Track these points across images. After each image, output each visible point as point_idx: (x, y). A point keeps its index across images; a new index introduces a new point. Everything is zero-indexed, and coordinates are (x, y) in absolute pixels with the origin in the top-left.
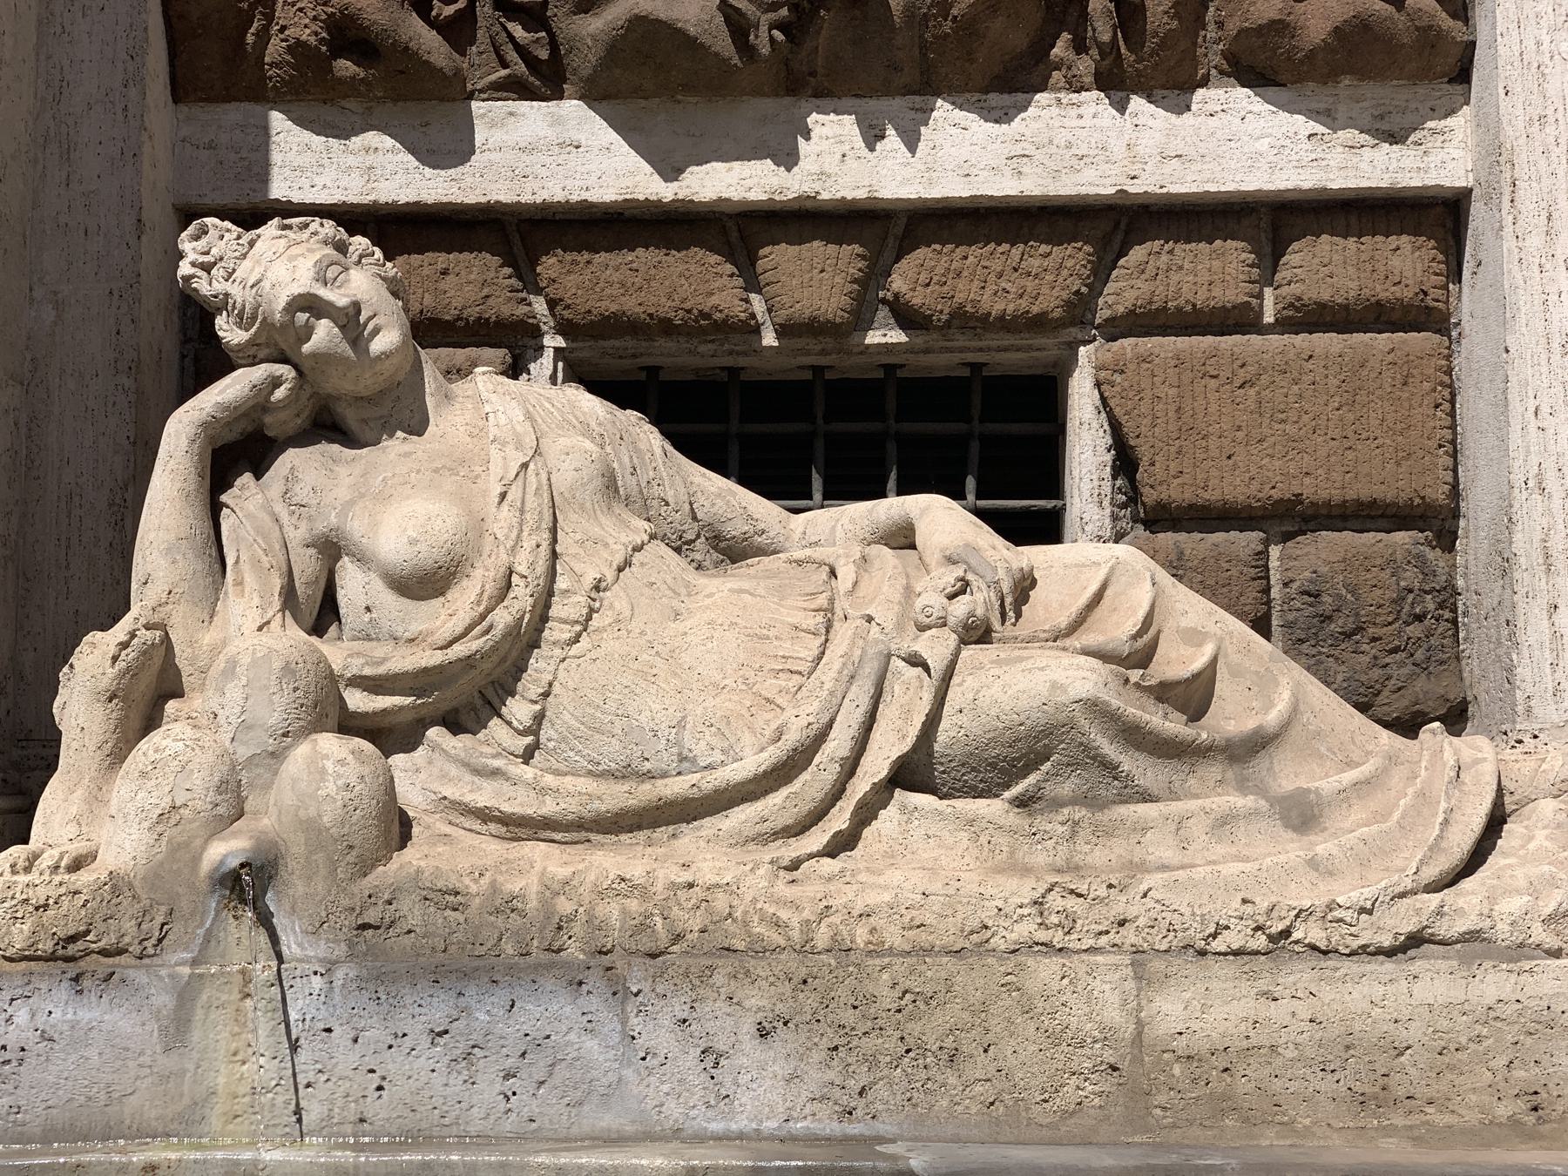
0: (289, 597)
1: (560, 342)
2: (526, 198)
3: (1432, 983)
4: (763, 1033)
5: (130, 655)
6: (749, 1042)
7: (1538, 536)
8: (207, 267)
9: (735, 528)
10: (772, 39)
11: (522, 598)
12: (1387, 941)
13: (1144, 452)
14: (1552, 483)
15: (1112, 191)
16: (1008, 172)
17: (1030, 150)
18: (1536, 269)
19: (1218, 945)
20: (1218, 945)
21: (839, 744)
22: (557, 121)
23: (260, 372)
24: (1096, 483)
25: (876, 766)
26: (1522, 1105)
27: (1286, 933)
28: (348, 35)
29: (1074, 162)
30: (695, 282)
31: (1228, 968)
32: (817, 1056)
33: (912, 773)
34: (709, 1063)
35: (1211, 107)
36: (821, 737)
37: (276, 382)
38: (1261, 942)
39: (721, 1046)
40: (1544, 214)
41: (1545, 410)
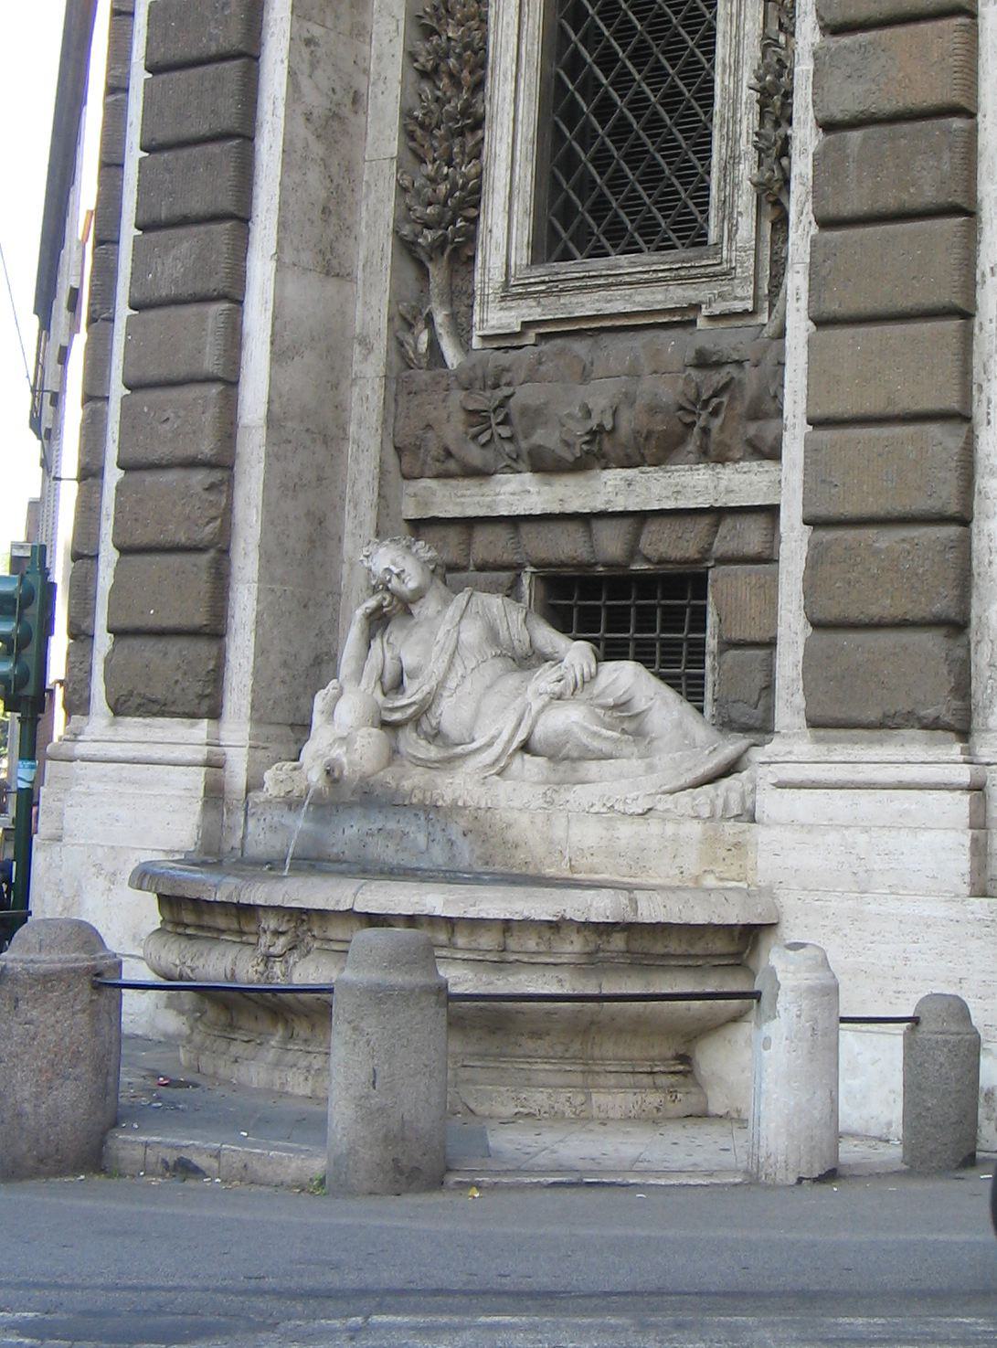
0: (381, 677)
1: (533, 570)
3: (654, 827)
4: (465, 835)
5: (328, 698)
6: (461, 837)
8: (367, 557)
9: (548, 650)
10: (581, 449)
11: (434, 683)
12: (641, 811)
15: (707, 506)
19: (592, 810)
20: (592, 810)
21: (505, 736)
22: (522, 483)
23: (379, 597)
25: (515, 744)
26: (677, 871)
27: (612, 806)
28: (449, 454)
30: (566, 546)
31: (595, 816)
32: (480, 843)
33: (525, 747)
35: (745, 469)
36: (500, 733)
37: (384, 599)
38: (604, 810)
39: (453, 838)
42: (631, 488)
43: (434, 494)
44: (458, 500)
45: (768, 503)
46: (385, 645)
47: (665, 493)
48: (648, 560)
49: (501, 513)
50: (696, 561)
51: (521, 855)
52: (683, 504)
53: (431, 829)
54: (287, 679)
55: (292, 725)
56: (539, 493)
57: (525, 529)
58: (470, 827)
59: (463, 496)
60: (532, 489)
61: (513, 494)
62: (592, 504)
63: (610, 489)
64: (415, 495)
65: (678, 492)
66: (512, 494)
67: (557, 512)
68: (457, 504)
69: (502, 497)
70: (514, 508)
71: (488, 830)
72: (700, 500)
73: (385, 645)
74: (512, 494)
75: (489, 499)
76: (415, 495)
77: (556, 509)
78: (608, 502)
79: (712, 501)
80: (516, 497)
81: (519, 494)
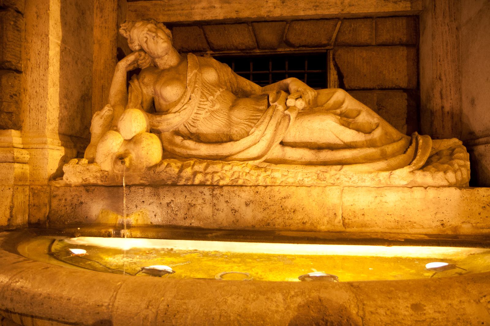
1: (212, 52)
2: (203, 19)
4: (247, 205)
7: (439, 90)
13: (345, 75)
14: (443, 77)
16: (313, 10)
17: (318, 4)
18: (440, 25)
24: (334, 82)
29: (329, 7)
34: (233, 211)
40: (442, 12)
41: (442, 59)
42: (285, 4)
43: (148, 10)
44: (165, 13)
45: (377, 11)
46: (141, 84)
47: (308, 6)
48: (289, 44)
49: (196, 19)
50: (325, 45)
51: (299, 217)
52: (320, 12)
53: (215, 201)
54: (68, 106)
55: (71, 136)
56: (221, 8)
57: (208, 28)
58: (252, 198)
59: (169, 10)
60: (216, 6)
61: (203, 8)
62: (258, 13)
63: (271, 5)
64: (136, 11)
65: (317, 6)
66: (203, 8)
67: (234, 17)
68: (164, 15)
69: (196, 10)
70: (204, 16)
71: (268, 201)
72: (332, 10)
73: (141, 84)
74: (203, 8)
75: (187, 12)
76: (136, 11)
77: (234, 15)
78: (270, 11)
79: (340, 10)
80: (206, 10)
81: (208, 8)
